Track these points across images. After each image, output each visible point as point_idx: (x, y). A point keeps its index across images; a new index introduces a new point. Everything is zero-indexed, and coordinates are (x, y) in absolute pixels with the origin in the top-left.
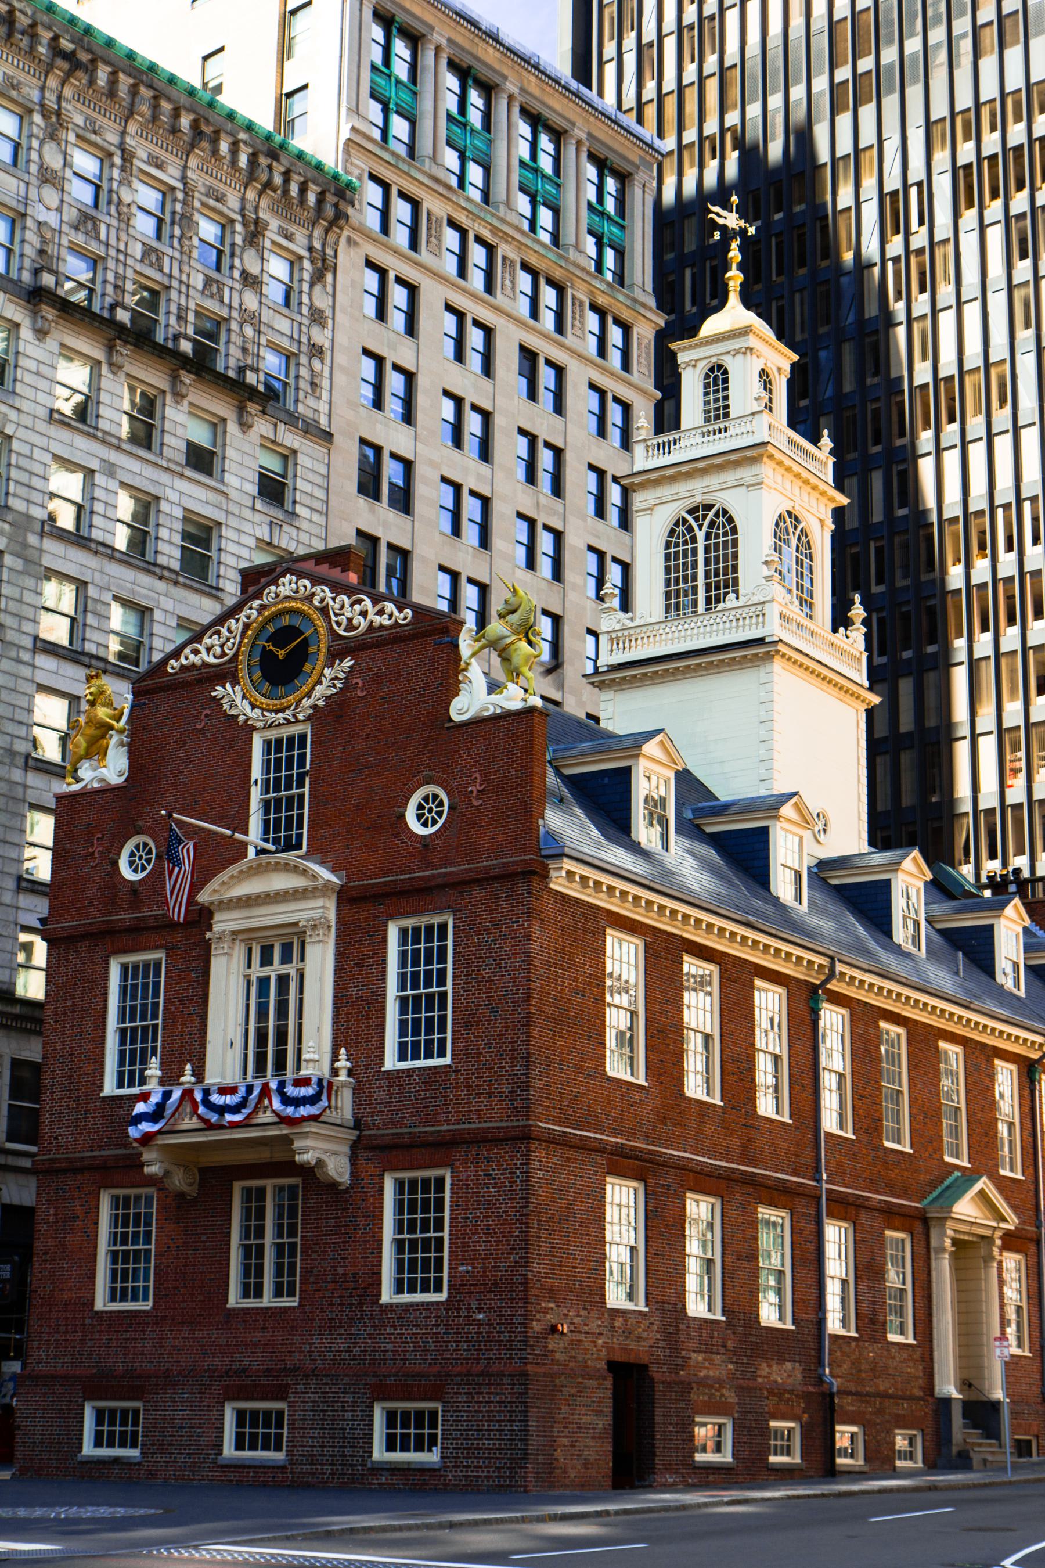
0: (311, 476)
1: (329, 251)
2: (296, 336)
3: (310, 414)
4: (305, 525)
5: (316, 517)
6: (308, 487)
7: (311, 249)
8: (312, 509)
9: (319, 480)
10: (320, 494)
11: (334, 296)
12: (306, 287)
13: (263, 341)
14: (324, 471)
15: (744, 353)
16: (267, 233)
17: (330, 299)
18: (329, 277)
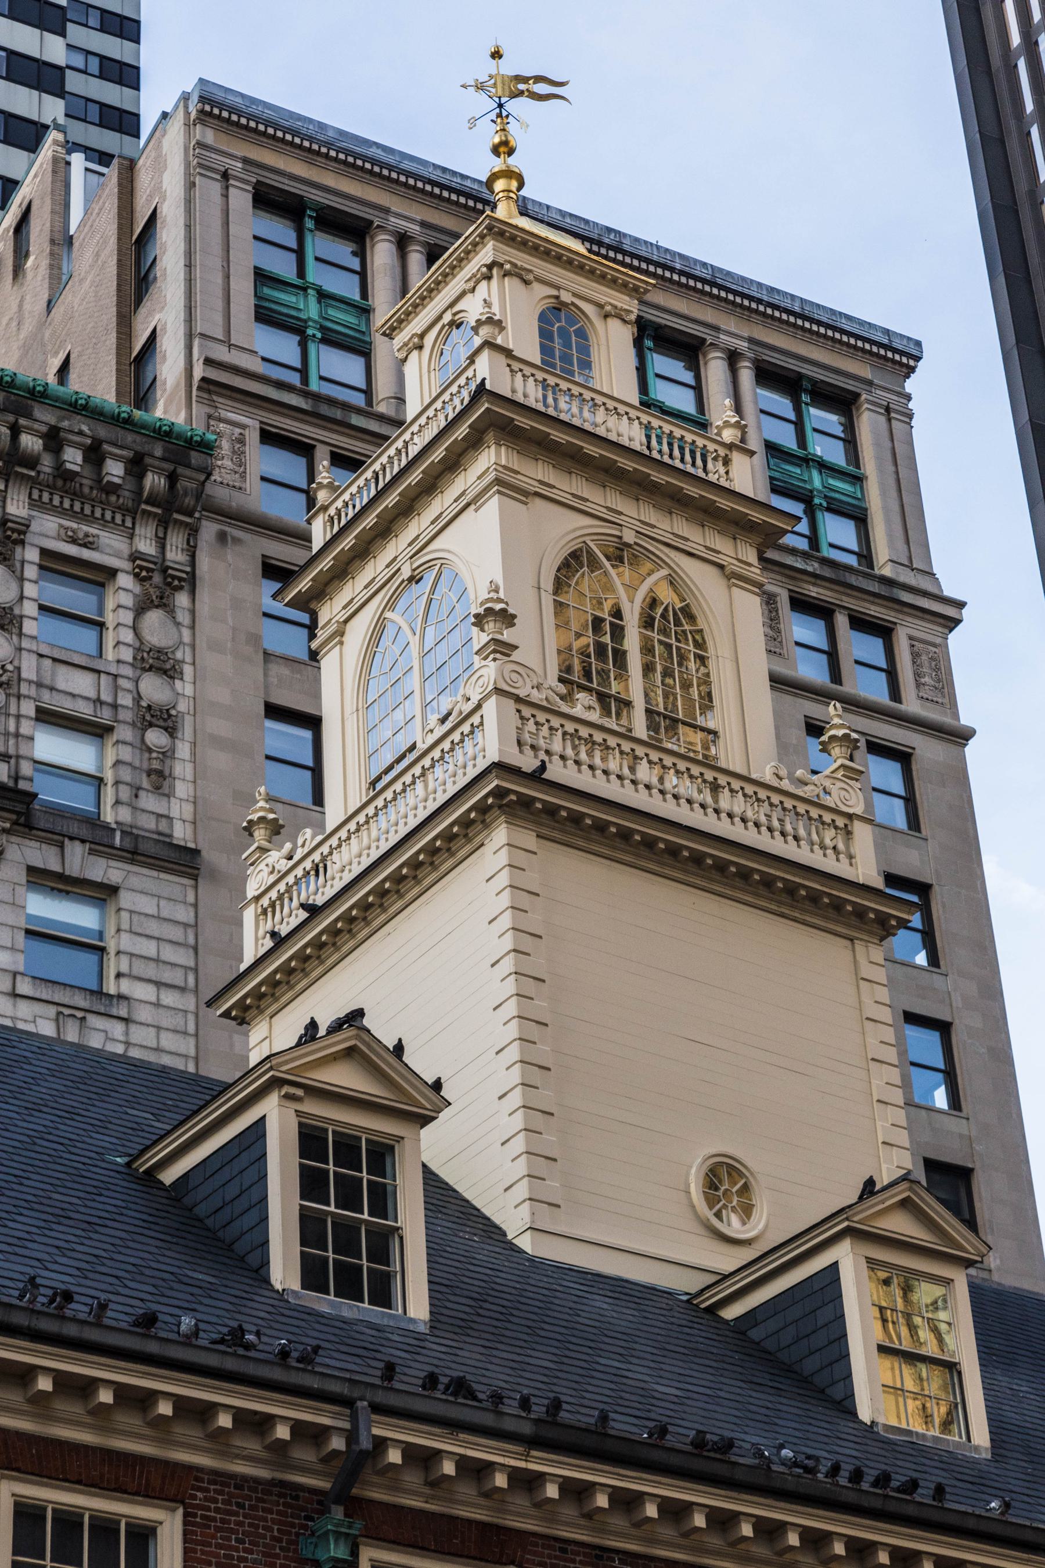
0: (153, 928)
1: (175, 555)
2: (106, 697)
3: (148, 823)
4: (143, 1014)
5: (169, 998)
6: (149, 948)
7: (135, 557)
8: (159, 984)
9: (176, 933)
10: (184, 958)
11: (193, 627)
12: (127, 617)
13: (28, 708)
14: (185, 915)
15: (489, 278)
16: (29, 538)
17: (186, 634)
18: (182, 599)
